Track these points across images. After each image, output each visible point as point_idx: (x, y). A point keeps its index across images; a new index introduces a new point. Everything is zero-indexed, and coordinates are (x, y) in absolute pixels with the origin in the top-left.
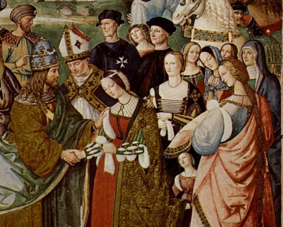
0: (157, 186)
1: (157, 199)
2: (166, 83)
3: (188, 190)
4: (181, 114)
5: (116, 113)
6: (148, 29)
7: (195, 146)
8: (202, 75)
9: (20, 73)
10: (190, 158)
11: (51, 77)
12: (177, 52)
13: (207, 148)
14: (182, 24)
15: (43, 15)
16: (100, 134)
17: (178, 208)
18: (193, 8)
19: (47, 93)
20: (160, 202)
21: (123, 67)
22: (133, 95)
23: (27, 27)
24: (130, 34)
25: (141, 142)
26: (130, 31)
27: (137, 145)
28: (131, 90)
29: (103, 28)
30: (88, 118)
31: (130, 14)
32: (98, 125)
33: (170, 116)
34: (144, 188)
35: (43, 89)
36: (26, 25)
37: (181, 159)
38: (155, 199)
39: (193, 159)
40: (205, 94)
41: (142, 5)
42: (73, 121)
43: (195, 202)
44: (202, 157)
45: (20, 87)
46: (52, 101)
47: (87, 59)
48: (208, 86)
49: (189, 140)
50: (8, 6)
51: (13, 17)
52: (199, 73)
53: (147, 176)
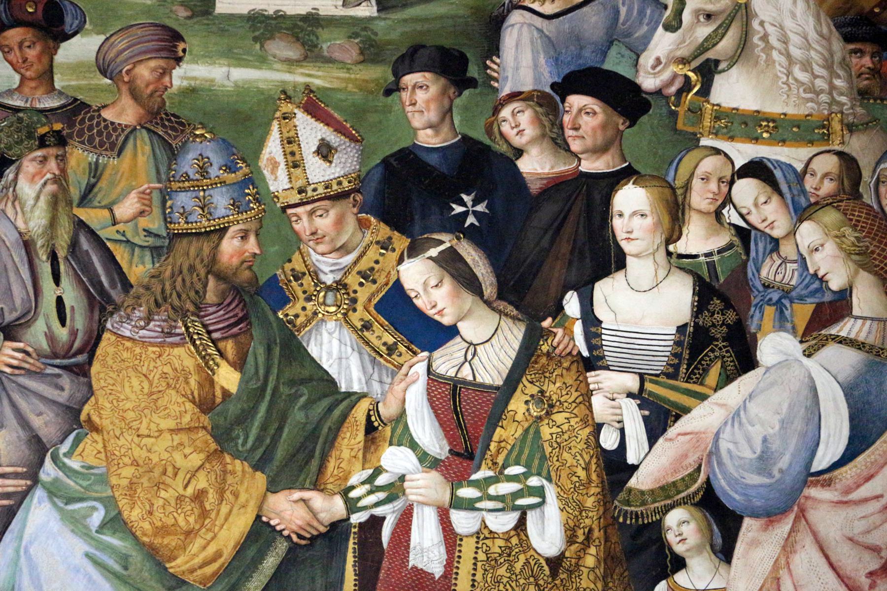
2: (619, 276)
4: (669, 376)
5: (451, 373)
6: (556, 103)
7: (721, 485)
8: (740, 250)
9: (128, 241)
10: (704, 524)
11: (232, 257)
13: (761, 490)
14: (673, 89)
15: (208, 57)
16: (395, 440)
19: (219, 305)
21: (472, 224)
22: (506, 315)
23: (151, 95)
24: (496, 119)
25: (534, 471)
26: (496, 111)
27: (522, 477)
28: (501, 296)
29: (407, 103)
30: (356, 388)
31: (494, 58)
32: (387, 410)
33: (631, 382)
35: (205, 292)
36: (151, 88)
37: (675, 528)
39: (715, 527)
40: (751, 312)
41: (537, 29)
42: (303, 400)
44: (747, 522)
45: (127, 286)
46: (235, 330)
47: (355, 200)
48: (761, 288)
49: (700, 466)
50: (87, 26)
51: (108, 58)
52: (730, 246)
53: (558, 582)
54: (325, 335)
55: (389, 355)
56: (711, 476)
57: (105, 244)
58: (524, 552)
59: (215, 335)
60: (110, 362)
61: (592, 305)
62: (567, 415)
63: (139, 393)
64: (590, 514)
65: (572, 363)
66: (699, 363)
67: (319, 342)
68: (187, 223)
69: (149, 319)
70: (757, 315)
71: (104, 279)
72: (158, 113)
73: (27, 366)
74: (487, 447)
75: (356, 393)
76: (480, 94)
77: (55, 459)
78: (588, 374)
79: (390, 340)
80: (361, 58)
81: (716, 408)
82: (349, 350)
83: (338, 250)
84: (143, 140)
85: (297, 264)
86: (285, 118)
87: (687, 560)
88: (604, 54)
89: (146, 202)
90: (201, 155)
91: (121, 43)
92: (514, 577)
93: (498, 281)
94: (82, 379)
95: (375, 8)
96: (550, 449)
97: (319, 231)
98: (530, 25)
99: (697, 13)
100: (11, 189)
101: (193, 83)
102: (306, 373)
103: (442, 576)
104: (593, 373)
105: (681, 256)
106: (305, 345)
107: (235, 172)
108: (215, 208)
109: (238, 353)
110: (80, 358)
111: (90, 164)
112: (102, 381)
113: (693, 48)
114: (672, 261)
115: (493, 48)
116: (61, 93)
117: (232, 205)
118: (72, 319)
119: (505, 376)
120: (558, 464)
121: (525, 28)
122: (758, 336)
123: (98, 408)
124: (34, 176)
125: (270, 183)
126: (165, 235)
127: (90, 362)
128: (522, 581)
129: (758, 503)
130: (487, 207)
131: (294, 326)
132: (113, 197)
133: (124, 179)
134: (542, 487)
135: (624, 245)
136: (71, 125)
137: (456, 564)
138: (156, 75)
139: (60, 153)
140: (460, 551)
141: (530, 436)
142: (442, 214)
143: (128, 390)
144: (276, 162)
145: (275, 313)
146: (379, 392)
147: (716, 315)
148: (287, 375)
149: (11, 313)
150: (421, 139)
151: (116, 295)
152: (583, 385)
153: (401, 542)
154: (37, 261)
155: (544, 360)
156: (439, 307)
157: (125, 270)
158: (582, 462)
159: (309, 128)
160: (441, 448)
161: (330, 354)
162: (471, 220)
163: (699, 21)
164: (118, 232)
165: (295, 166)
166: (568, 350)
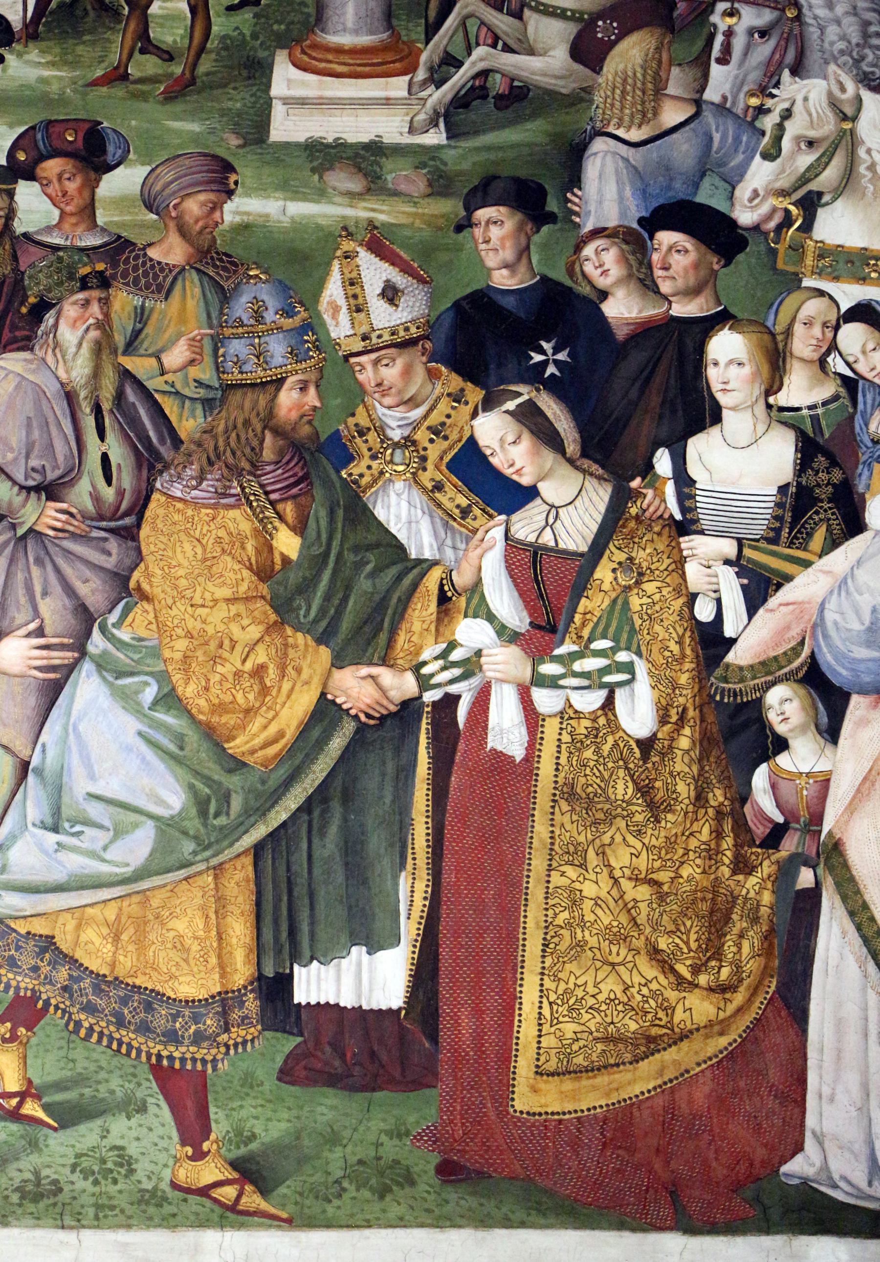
0: (687, 801)
1: (687, 851)
2: (715, 431)
3: (802, 820)
4: (770, 541)
5: (532, 538)
6: (644, 241)
7: (827, 660)
8: (847, 402)
9: (177, 393)
10: (808, 702)
11: (290, 410)
12: (751, 322)
13: (870, 664)
14: (772, 225)
15: (261, 190)
16: (470, 612)
17: (769, 885)
18: (808, 169)
19: (277, 463)
20: (698, 861)
21: (552, 375)
22: (591, 474)
23: (200, 233)
24: (578, 258)
25: (623, 645)
26: (578, 249)
27: (610, 653)
28: (584, 454)
29: (480, 241)
30: (427, 555)
31: (576, 190)
32: (461, 579)
33: (729, 548)
34: (639, 809)
35: (262, 449)
36: (200, 224)
37: (777, 706)
38: (681, 852)
39: (820, 705)
40: (859, 471)
41: (622, 157)
42: (369, 567)
43: (834, 861)
44: (855, 699)
45: (177, 442)
46: (295, 491)
47: (423, 348)
48: (870, 444)
49: (804, 639)
50: (131, 156)
51: (153, 193)
52: (835, 398)
53: (650, 765)
54: (393, 497)
55: (463, 518)
56: (816, 650)
57: (152, 396)
58: (612, 733)
59: (273, 496)
60: (160, 526)
61: (685, 463)
62: (659, 584)
63: (191, 558)
64: (684, 692)
65: (664, 527)
66: (803, 526)
67: (386, 504)
68: (241, 372)
69: (201, 479)
70: (866, 473)
71: (152, 434)
72: (208, 251)
73: (71, 528)
74: (571, 620)
75: (427, 560)
76: (561, 230)
77: (103, 630)
78: (681, 539)
79: (464, 502)
80: (429, 191)
81: (822, 577)
82: (419, 512)
83: (405, 403)
84: (192, 282)
85: (361, 418)
86: (346, 257)
87: (790, 742)
88: (696, 186)
89: (197, 350)
90: (255, 298)
91: (167, 175)
92: (601, 760)
93: (581, 437)
94: (130, 544)
95: (444, 135)
96: (640, 621)
97: (385, 382)
98: (615, 154)
99: (798, 139)
100: (51, 335)
101: (245, 218)
102: (372, 538)
103: (523, 760)
104: (687, 538)
105: (782, 409)
106: (371, 507)
107: (292, 317)
108: (272, 357)
109: (298, 516)
110: (128, 521)
111: (136, 308)
112: (152, 546)
113: (793, 179)
114: (772, 414)
115: (575, 180)
116: (103, 230)
117: (291, 353)
118: (119, 479)
119: (590, 542)
120: (648, 638)
121: (609, 158)
122: (867, 496)
123: (149, 576)
124: (75, 322)
125: (331, 329)
126: (217, 386)
127: (139, 526)
128: (610, 765)
129: (866, 679)
130: (568, 355)
131: (359, 487)
132: (160, 345)
133: (172, 324)
134: (632, 663)
135: (719, 396)
136: (115, 264)
137: (538, 747)
138: (205, 209)
139: (103, 296)
140: (542, 732)
141: (618, 607)
142: (519, 364)
143: (179, 556)
144: (337, 306)
145: (338, 472)
146: (453, 559)
147: (820, 474)
148: (352, 540)
149: (53, 470)
150: (495, 280)
151: (165, 451)
152: (675, 551)
153: (479, 723)
154: (79, 415)
155: (632, 524)
156: (518, 466)
157: (175, 424)
158: (674, 635)
159: (373, 267)
160: (520, 620)
161: (398, 517)
162: (551, 370)
163: (800, 148)
164: (166, 382)
165: (358, 310)
166: (659, 513)
